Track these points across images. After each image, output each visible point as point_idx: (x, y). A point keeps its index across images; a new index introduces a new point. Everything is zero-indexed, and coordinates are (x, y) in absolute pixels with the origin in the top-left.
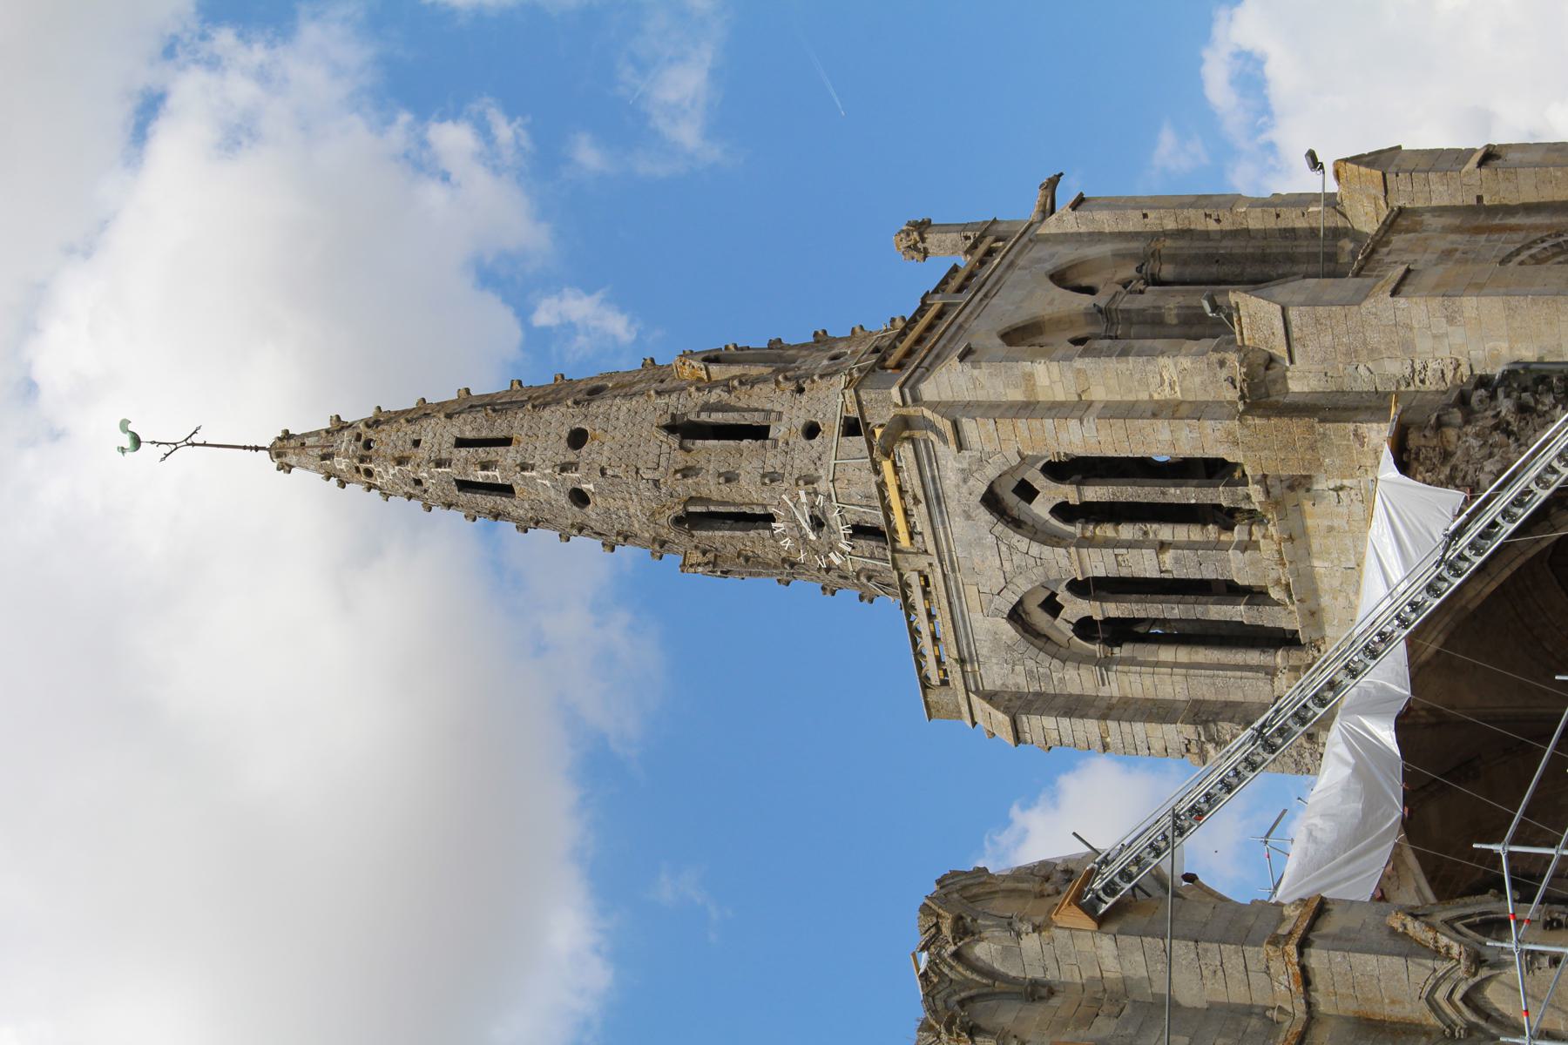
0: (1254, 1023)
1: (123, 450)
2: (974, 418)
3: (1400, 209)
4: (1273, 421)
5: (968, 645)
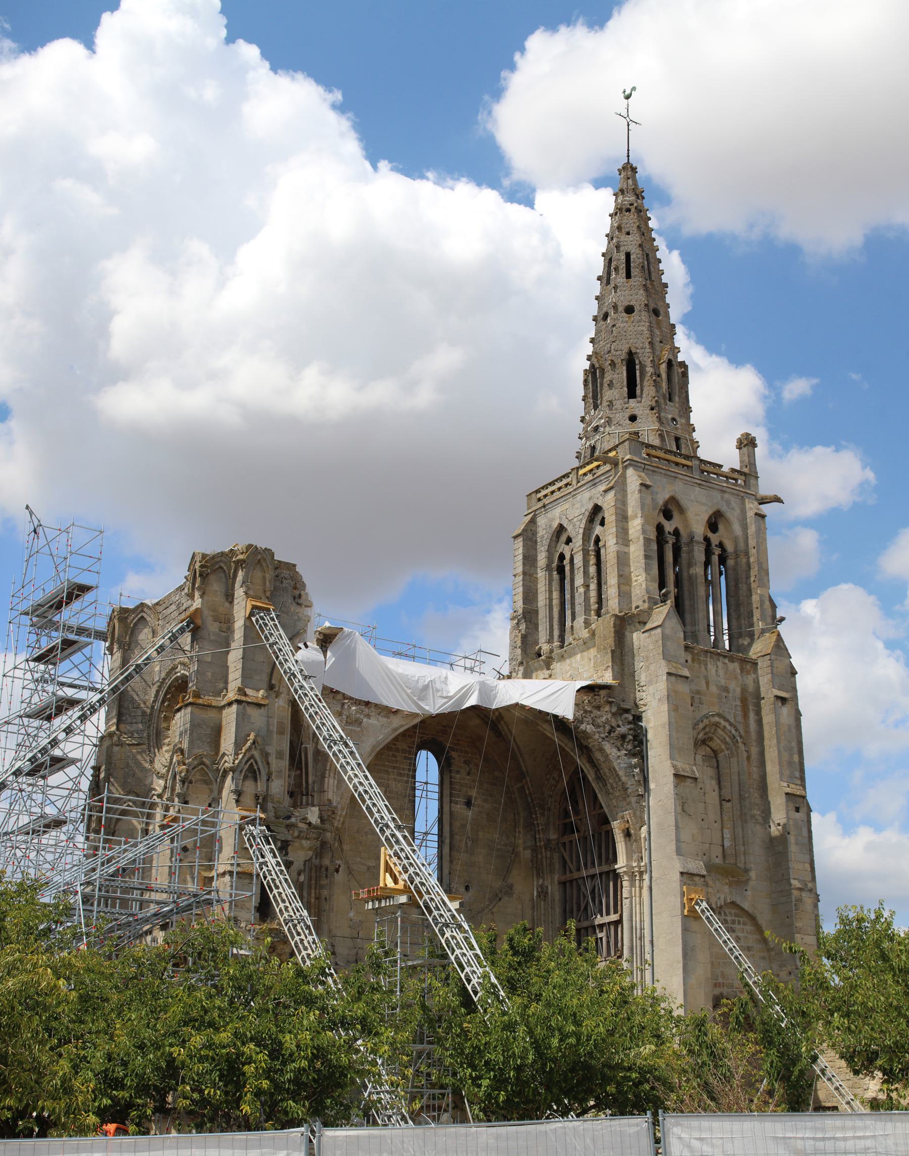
0: (222, 685)
1: (624, 92)
2: (615, 496)
3: (757, 664)
4: (612, 630)
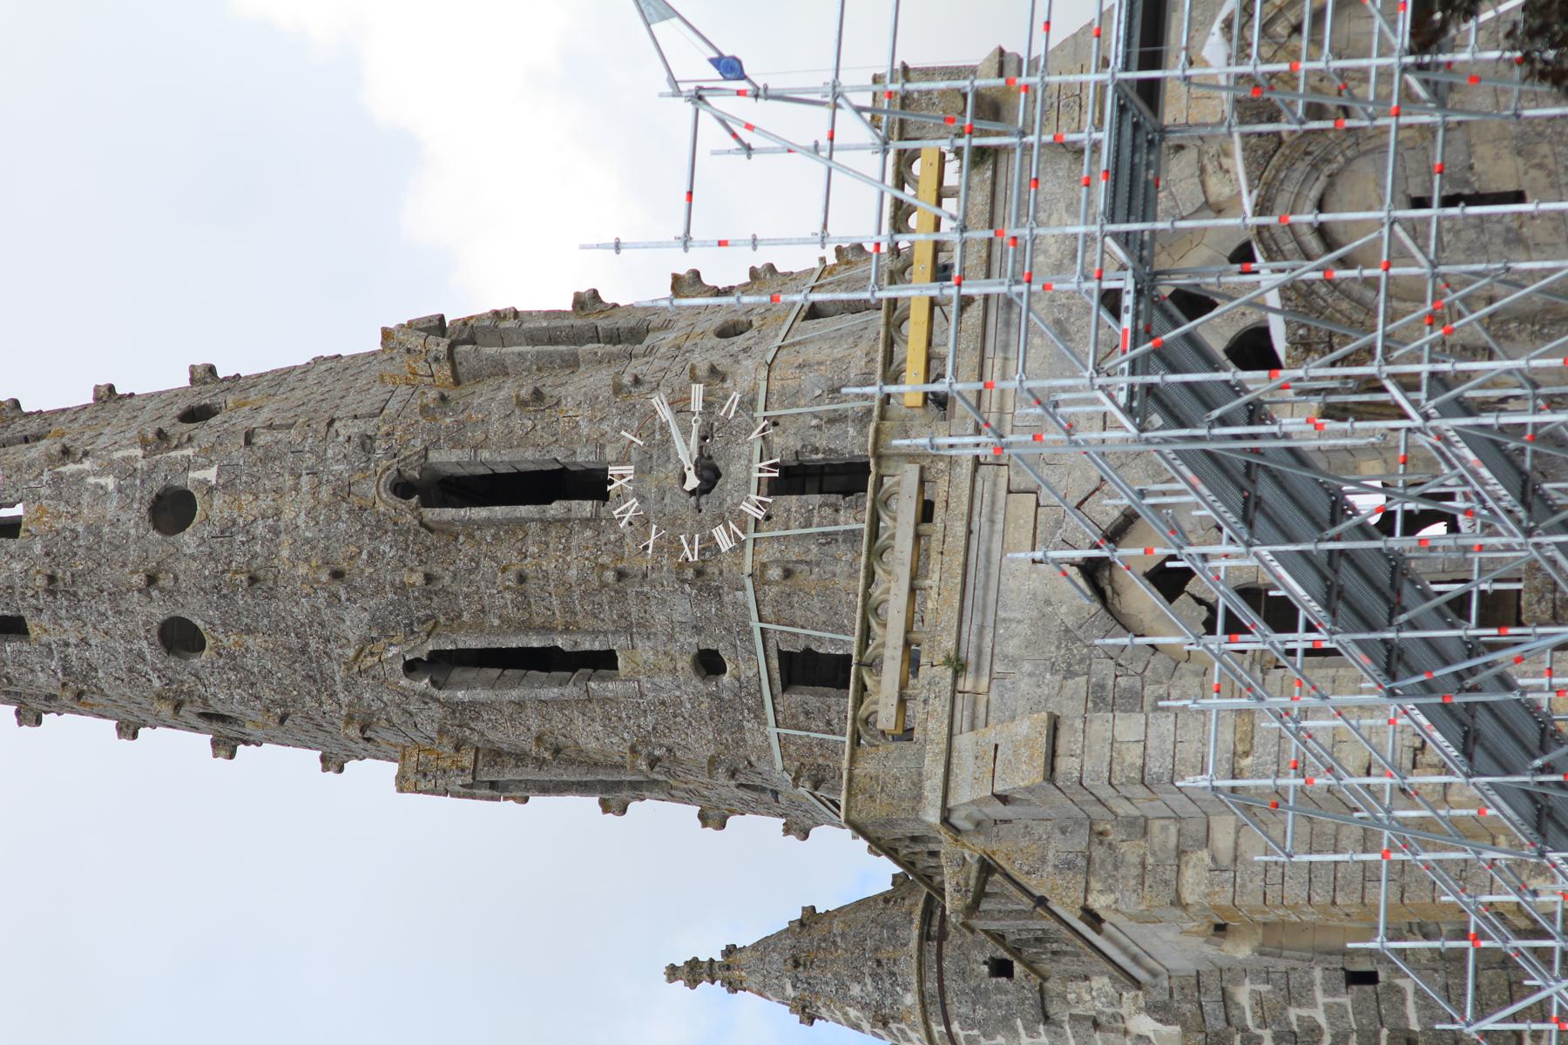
5: (982, 628)
